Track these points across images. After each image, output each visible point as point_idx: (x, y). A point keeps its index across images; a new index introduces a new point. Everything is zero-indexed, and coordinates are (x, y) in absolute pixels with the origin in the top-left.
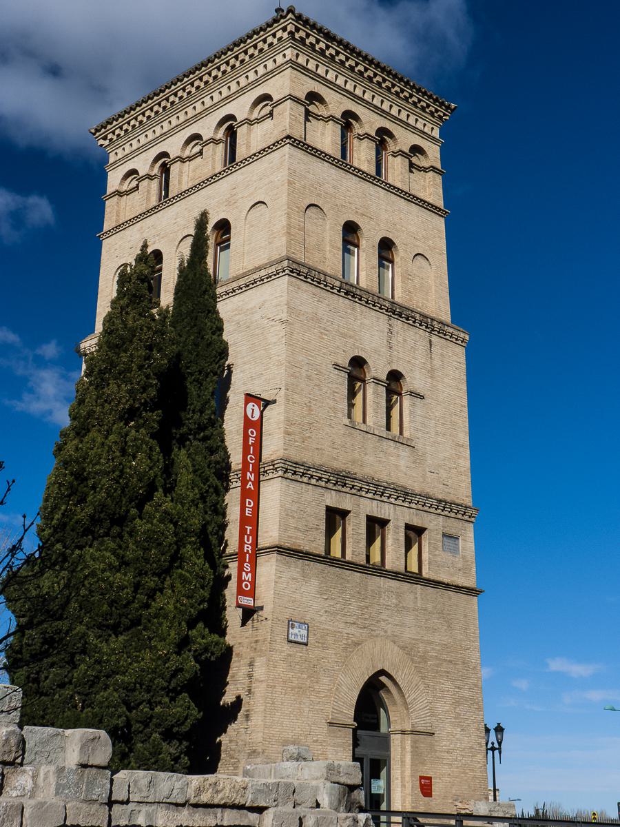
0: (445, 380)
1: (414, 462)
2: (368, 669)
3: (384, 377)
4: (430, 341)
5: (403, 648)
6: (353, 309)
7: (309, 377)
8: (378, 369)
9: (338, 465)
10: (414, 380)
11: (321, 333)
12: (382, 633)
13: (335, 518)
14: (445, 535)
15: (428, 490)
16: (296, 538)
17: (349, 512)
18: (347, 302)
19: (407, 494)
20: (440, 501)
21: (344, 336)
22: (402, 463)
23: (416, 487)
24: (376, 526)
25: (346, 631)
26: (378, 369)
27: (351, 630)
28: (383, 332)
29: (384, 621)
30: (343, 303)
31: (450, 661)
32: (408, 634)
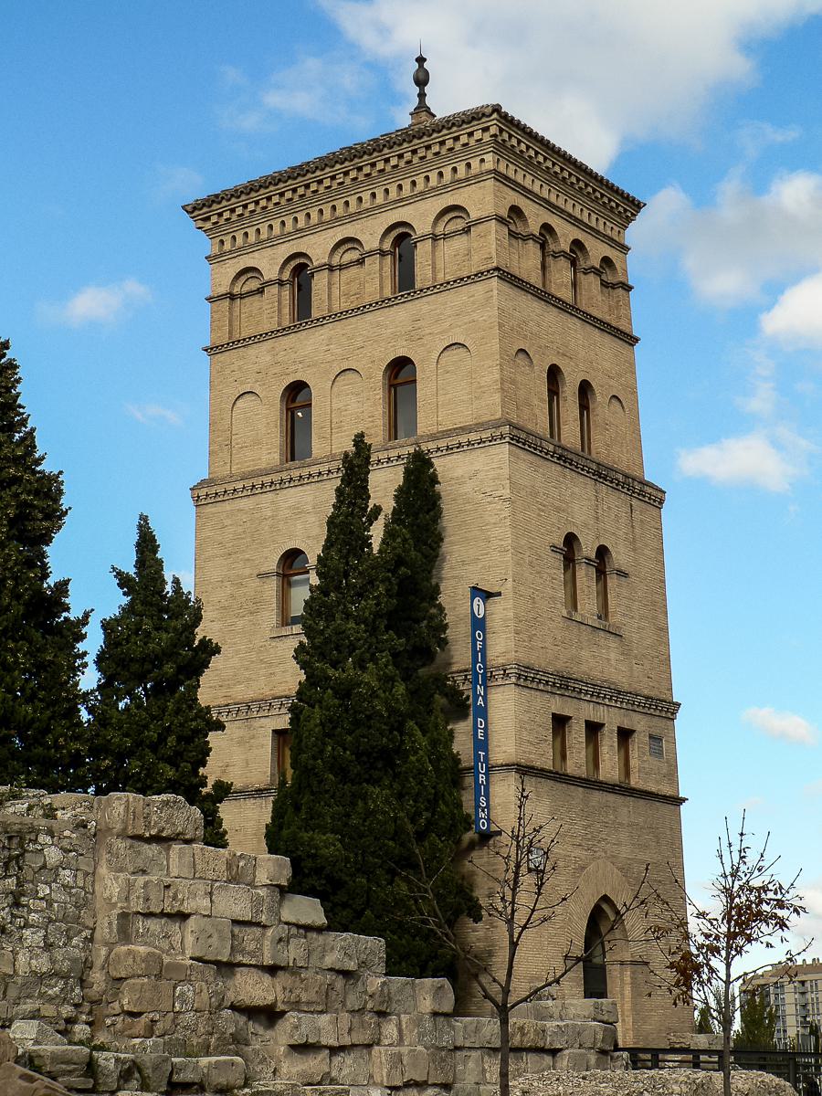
0: (646, 552)
1: (623, 654)
2: (593, 896)
3: (593, 556)
4: (631, 505)
5: (621, 869)
6: (565, 476)
7: (531, 564)
8: (588, 548)
9: (559, 665)
10: (620, 557)
11: (539, 509)
12: (603, 854)
13: (560, 722)
14: (650, 737)
15: (636, 687)
16: (530, 753)
17: (570, 718)
18: (559, 468)
19: (619, 692)
20: (647, 698)
21: (558, 510)
22: (613, 656)
23: (623, 682)
24: (593, 729)
25: (573, 855)
26: (588, 548)
27: (578, 852)
28: (589, 500)
29: (604, 840)
30: (554, 469)
31: (660, 882)
32: (625, 852)
